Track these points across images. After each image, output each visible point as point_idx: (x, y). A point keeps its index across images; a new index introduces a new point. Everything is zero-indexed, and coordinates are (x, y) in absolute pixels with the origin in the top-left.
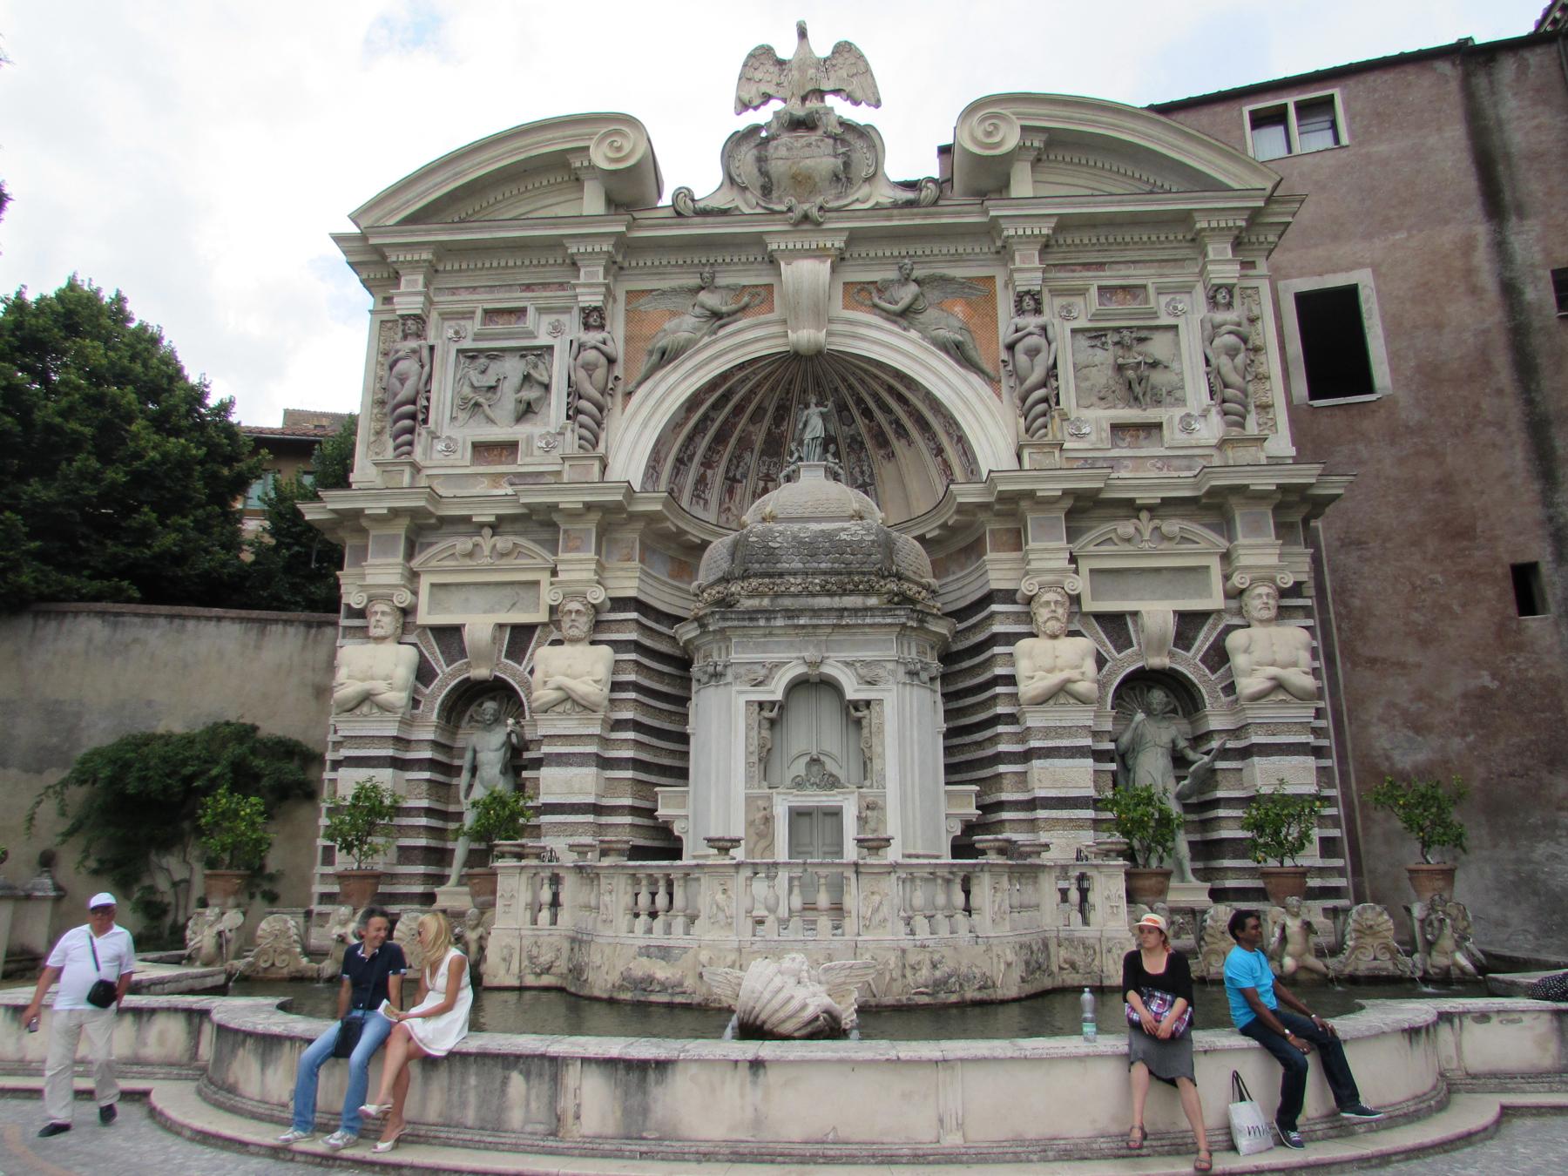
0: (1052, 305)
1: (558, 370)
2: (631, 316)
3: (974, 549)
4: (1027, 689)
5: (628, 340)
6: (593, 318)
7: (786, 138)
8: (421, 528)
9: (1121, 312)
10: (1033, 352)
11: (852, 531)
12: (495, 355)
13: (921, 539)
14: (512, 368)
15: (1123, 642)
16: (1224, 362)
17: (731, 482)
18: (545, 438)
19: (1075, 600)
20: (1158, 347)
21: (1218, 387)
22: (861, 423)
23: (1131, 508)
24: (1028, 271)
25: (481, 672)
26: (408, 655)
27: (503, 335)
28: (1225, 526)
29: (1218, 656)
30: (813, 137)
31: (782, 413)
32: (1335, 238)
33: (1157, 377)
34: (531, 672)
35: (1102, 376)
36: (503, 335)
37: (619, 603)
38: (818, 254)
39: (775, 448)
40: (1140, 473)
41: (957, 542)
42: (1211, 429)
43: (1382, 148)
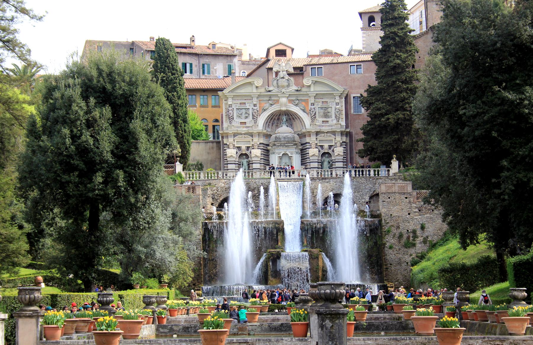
0: (316, 104)
1: (250, 112)
2: (260, 104)
3: (305, 136)
4: (310, 155)
5: (260, 107)
6: (255, 105)
7: (281, 80)
8: (235, 135)
9: (325, 105)
10: (313, 111)
11: (290, 135)
12: (241, 109)
13: (298, 135)
14: (244, 111)
15: (322, 149)
16: (337, 113)
17: (273, 124)
18: (249, 121)
19: (316, 144)
20: (329, 110)
21: (336, 116)
22: (291, 117)
23: (323, 132)
24: (312, 100)
25: (244, 153)
26: (235, 150)
27: (243, 106)
28: (335, 135)
29: (333, 151)
30: (284, 80)
31: (280, 115)
32: (359, 88)
33: (329, 114)
34: (250, 152)
35: (322, 114)
36: (243, 106)
37: (260, 144)
38: (285, 97)
39: (278, 119)
40: (325, 129)
41: (302, 135)
42: (335, 122)
43: (367, 75)
